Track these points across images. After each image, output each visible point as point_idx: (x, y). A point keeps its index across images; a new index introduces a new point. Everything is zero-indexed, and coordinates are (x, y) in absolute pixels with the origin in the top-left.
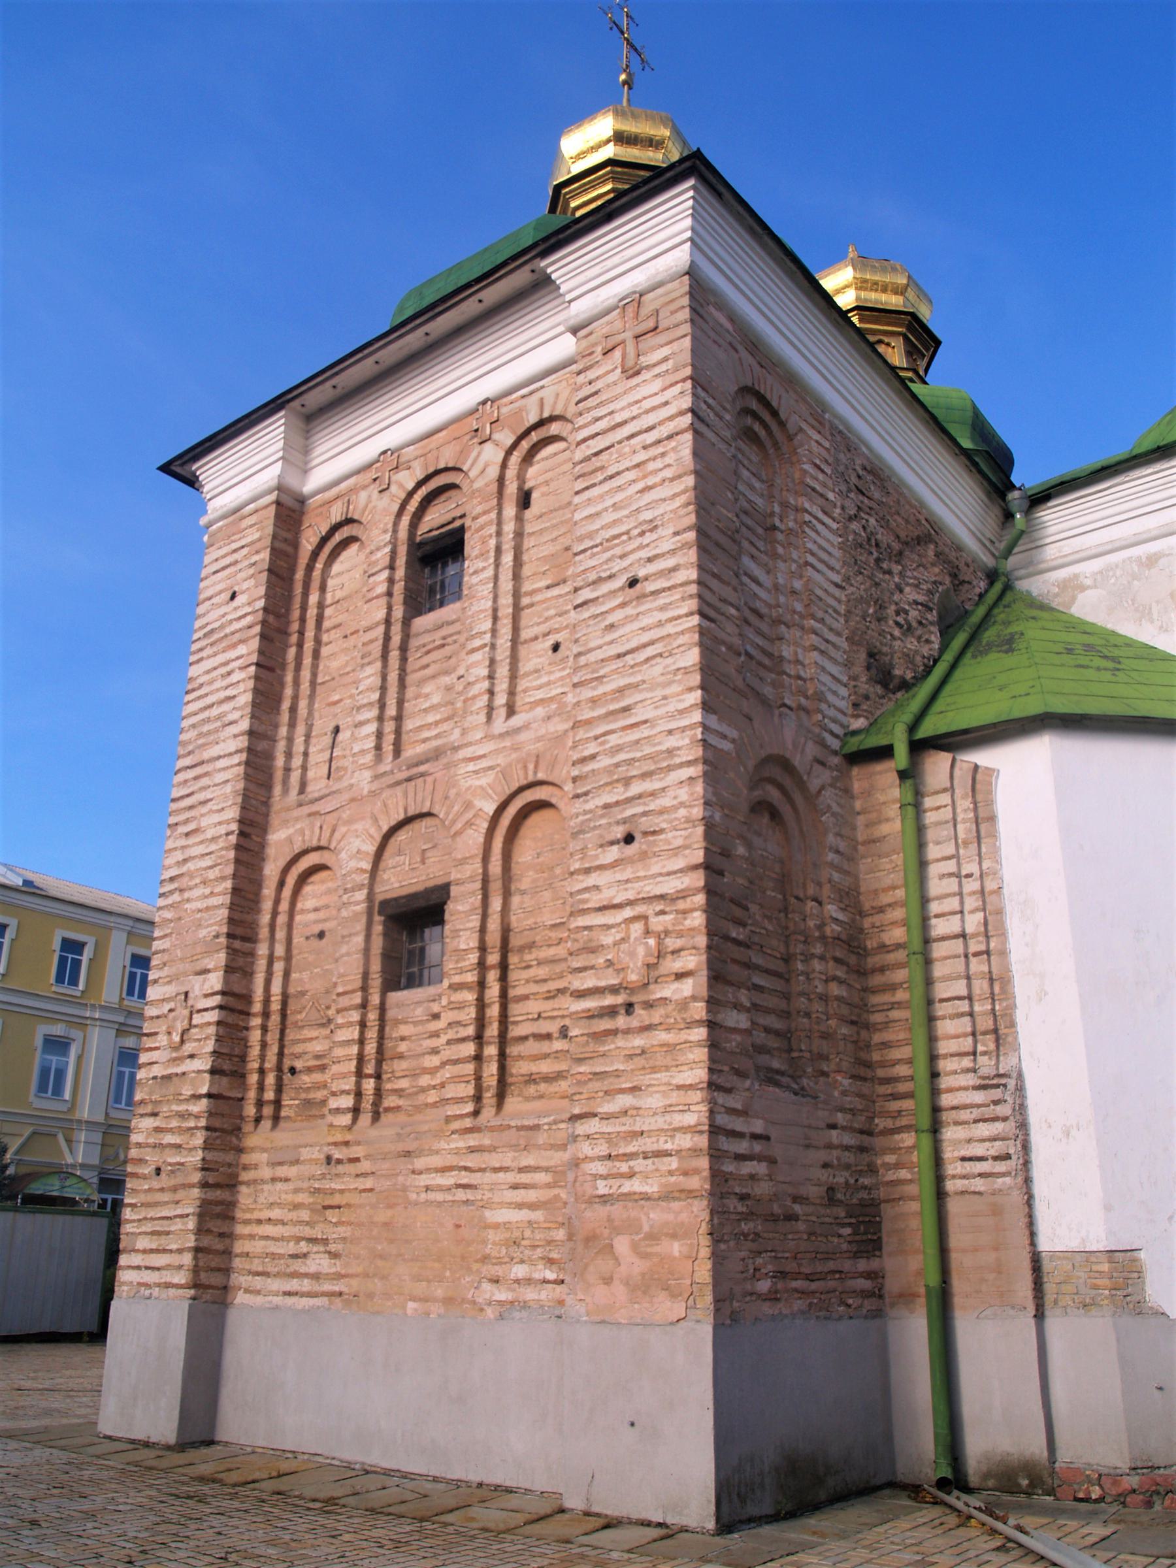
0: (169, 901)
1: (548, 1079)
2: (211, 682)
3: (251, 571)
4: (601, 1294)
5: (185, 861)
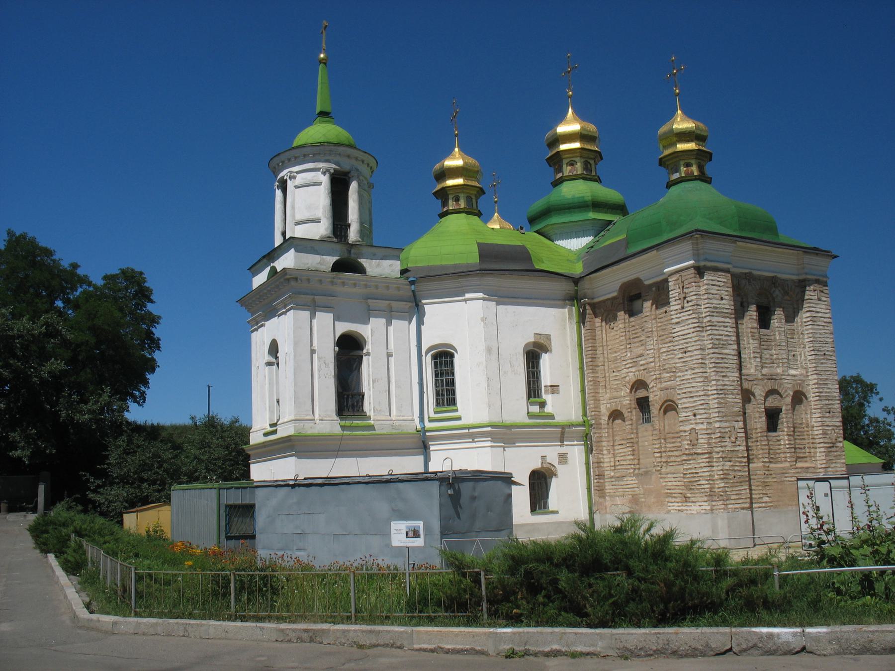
5: (725, 385)
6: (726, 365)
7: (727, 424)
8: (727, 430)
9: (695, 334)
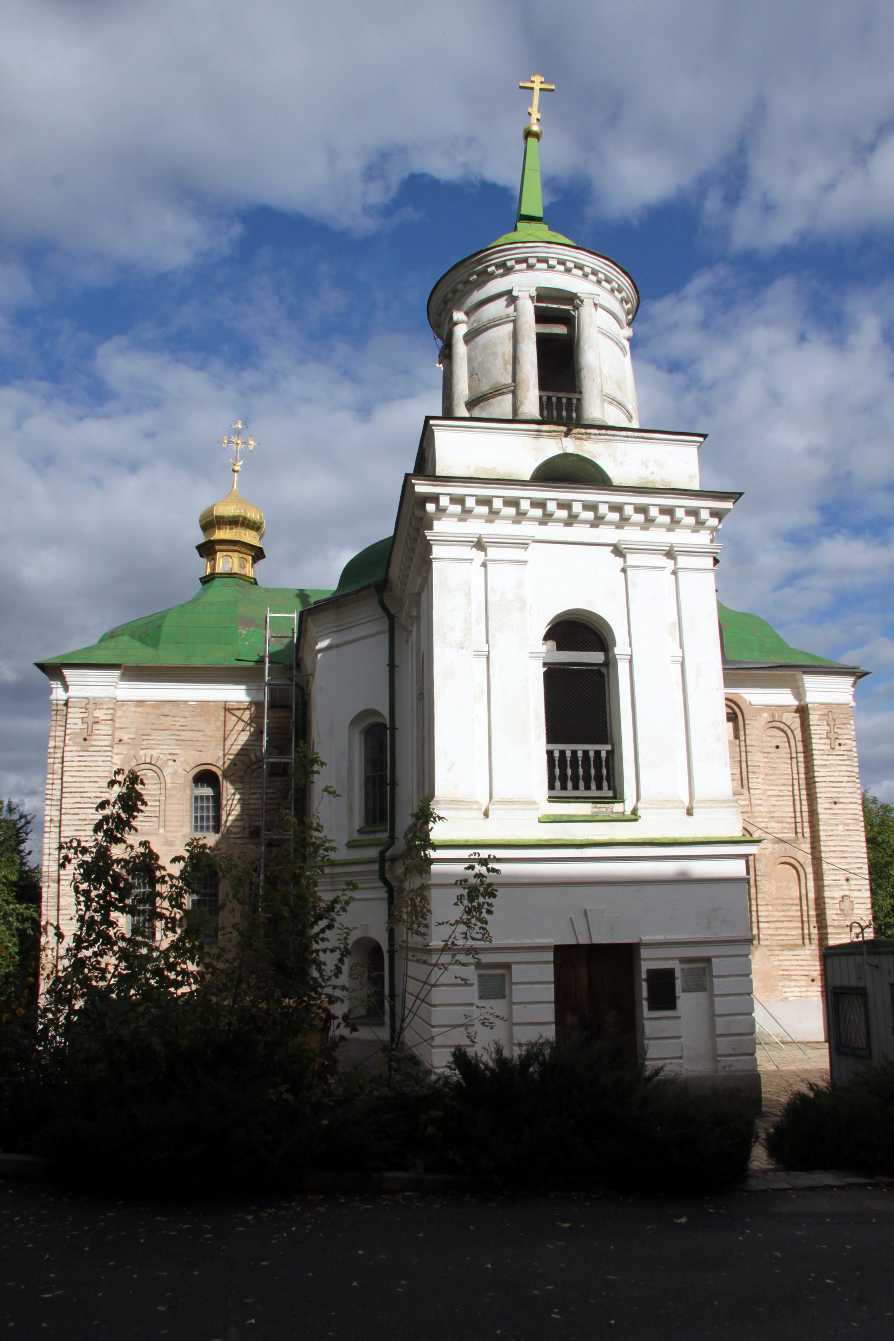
9: (851, 784)
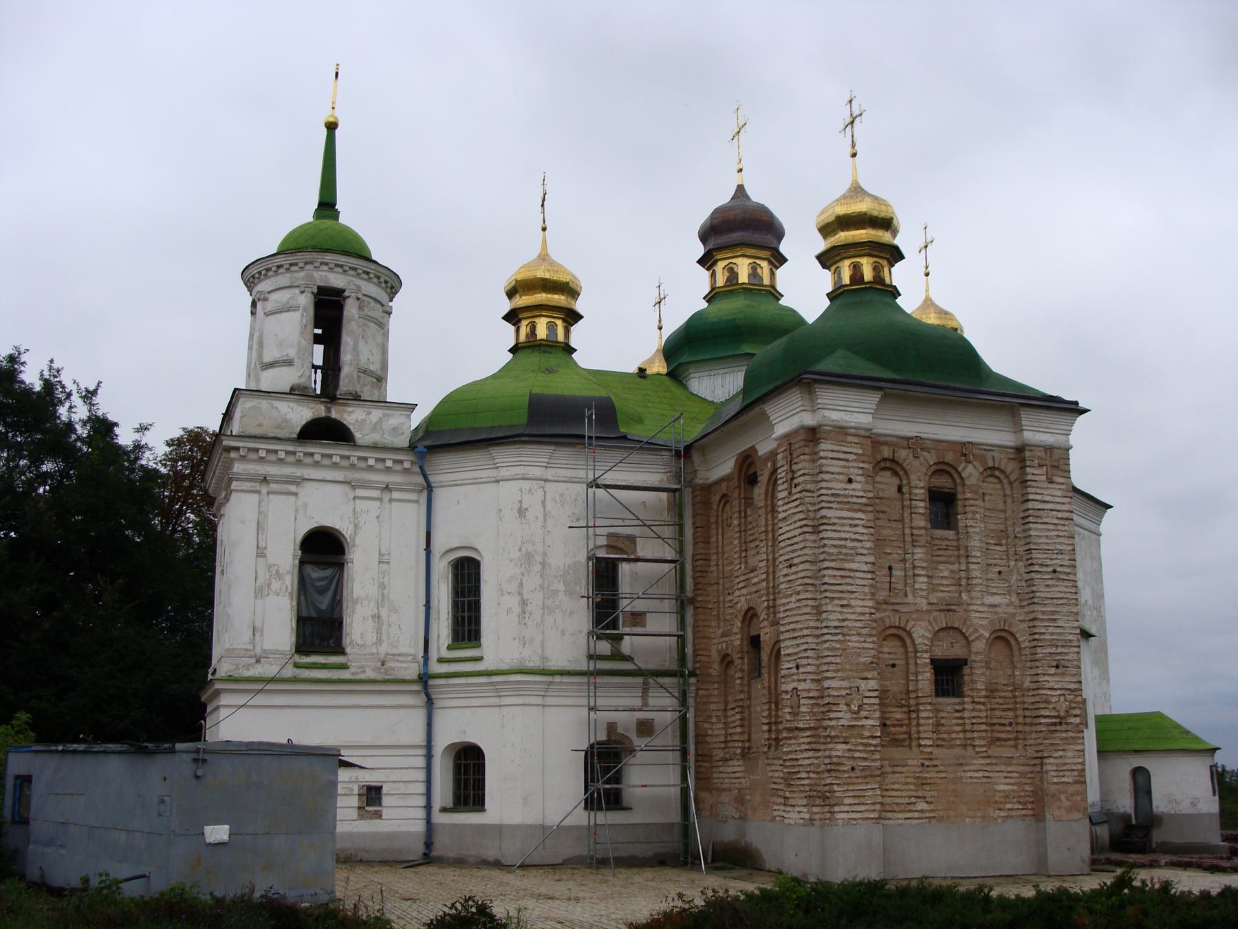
0: (836, 638)
1: (1005, 740)
2: (842, 525)
3: (861, 472)
4: (1057, 813)
5: (844, 620)
6: (849, 588)
7: (845, 684)
8: (844, 693)
